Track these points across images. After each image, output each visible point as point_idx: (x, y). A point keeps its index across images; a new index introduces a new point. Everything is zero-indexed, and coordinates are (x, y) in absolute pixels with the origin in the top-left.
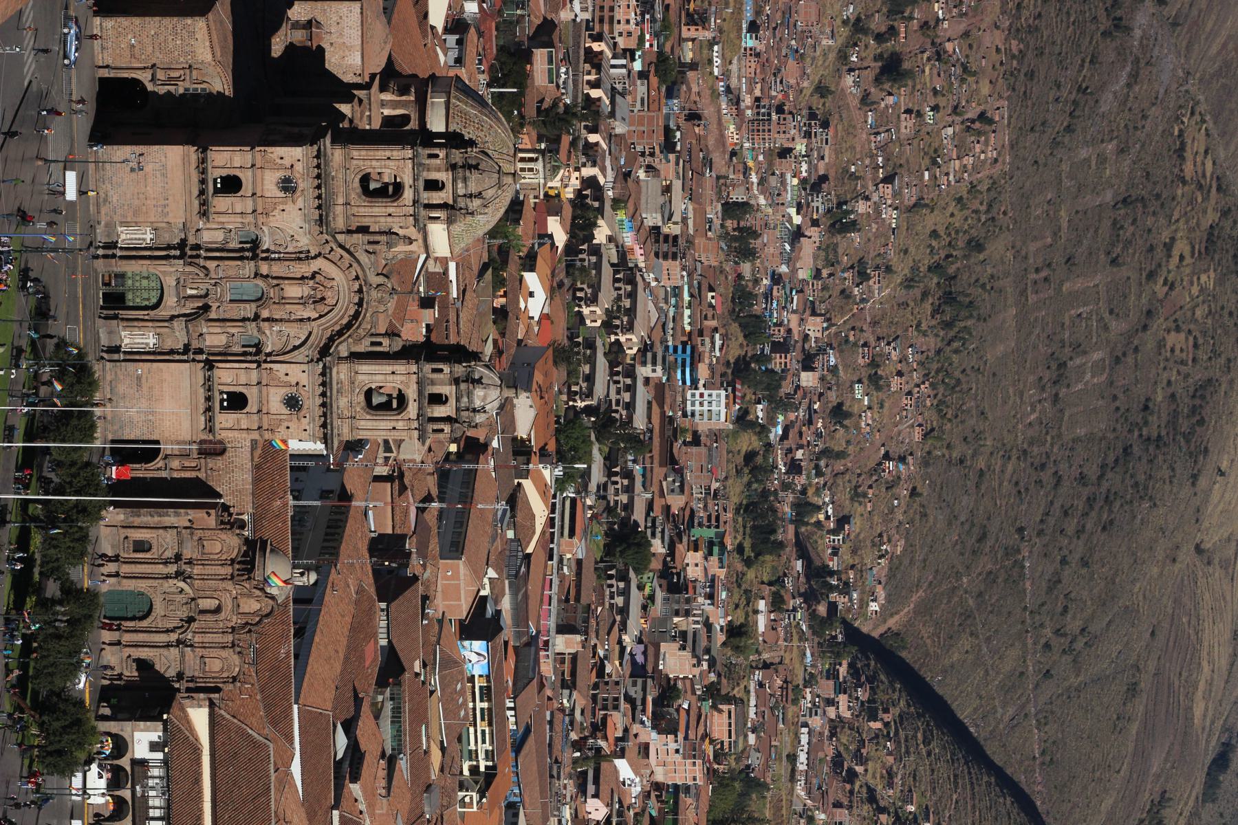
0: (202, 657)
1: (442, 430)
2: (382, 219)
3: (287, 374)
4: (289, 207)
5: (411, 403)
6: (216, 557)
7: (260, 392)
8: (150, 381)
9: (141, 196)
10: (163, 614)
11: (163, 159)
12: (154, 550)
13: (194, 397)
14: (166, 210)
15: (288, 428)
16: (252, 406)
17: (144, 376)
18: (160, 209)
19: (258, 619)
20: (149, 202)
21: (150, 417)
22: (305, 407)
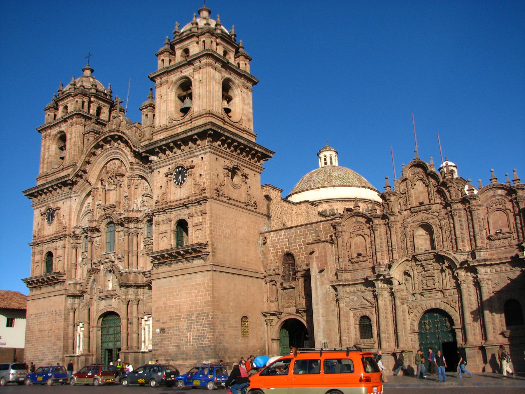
0: (489, 238)
1: (204, 42)
2: (73, 140)
3: (161, 186)
4: (61, 212)
5: (183, 75)
6: (368, 240)
7: (171, 208)
8: (165, 320)
9: (50, 335)
10: (440, 295)
11: (33, 317)
12: (367, 313)
13: (176, 273)
14: (58, 311)
15: (201, 175)
16: (183, 214)
17: (162, 326)
18: (58, 318)
19: (432, 181)
20: (53, 328)
21: (194, 317)
22: (183, 163)
